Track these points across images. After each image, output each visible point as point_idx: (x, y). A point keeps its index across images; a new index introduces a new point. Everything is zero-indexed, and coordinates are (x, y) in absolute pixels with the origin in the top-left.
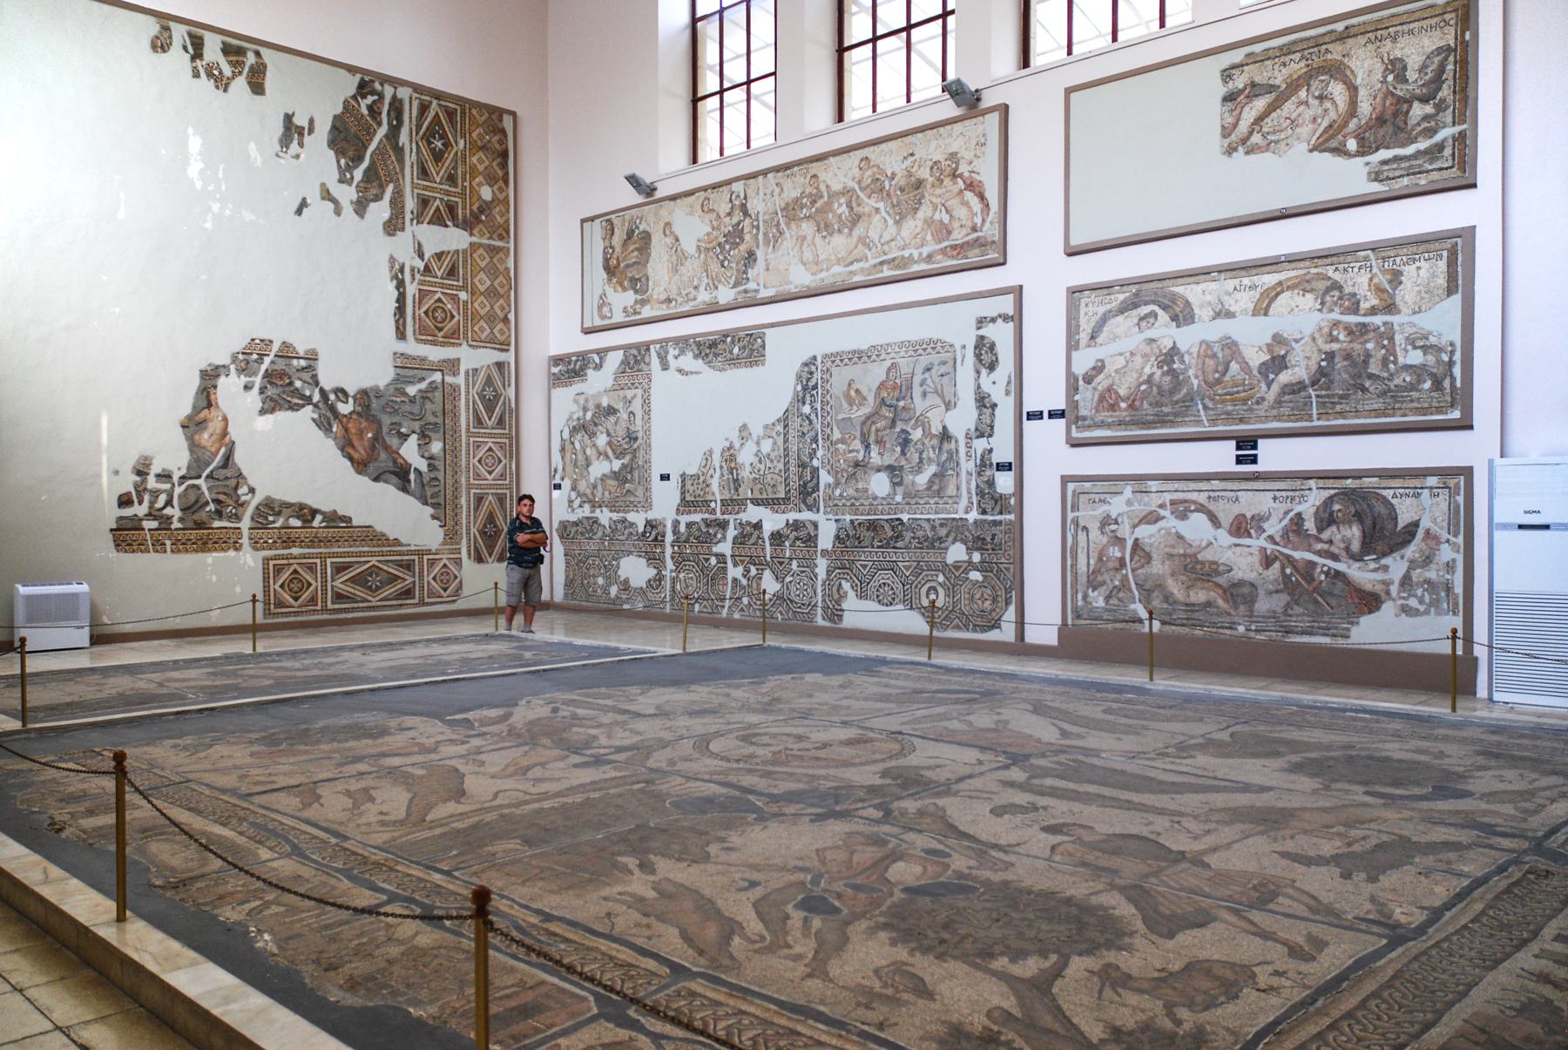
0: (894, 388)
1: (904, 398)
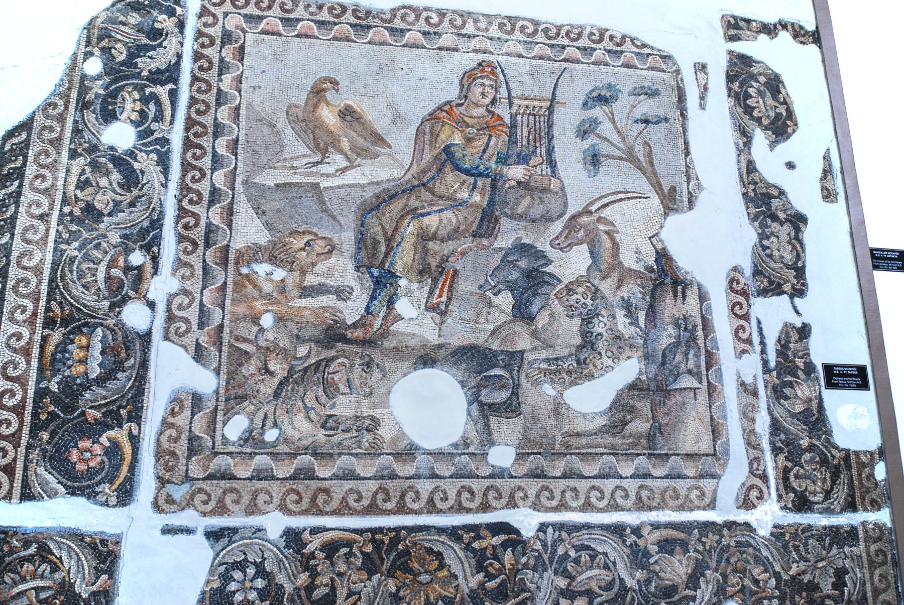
0: (488, 128)
1: (523, 159)
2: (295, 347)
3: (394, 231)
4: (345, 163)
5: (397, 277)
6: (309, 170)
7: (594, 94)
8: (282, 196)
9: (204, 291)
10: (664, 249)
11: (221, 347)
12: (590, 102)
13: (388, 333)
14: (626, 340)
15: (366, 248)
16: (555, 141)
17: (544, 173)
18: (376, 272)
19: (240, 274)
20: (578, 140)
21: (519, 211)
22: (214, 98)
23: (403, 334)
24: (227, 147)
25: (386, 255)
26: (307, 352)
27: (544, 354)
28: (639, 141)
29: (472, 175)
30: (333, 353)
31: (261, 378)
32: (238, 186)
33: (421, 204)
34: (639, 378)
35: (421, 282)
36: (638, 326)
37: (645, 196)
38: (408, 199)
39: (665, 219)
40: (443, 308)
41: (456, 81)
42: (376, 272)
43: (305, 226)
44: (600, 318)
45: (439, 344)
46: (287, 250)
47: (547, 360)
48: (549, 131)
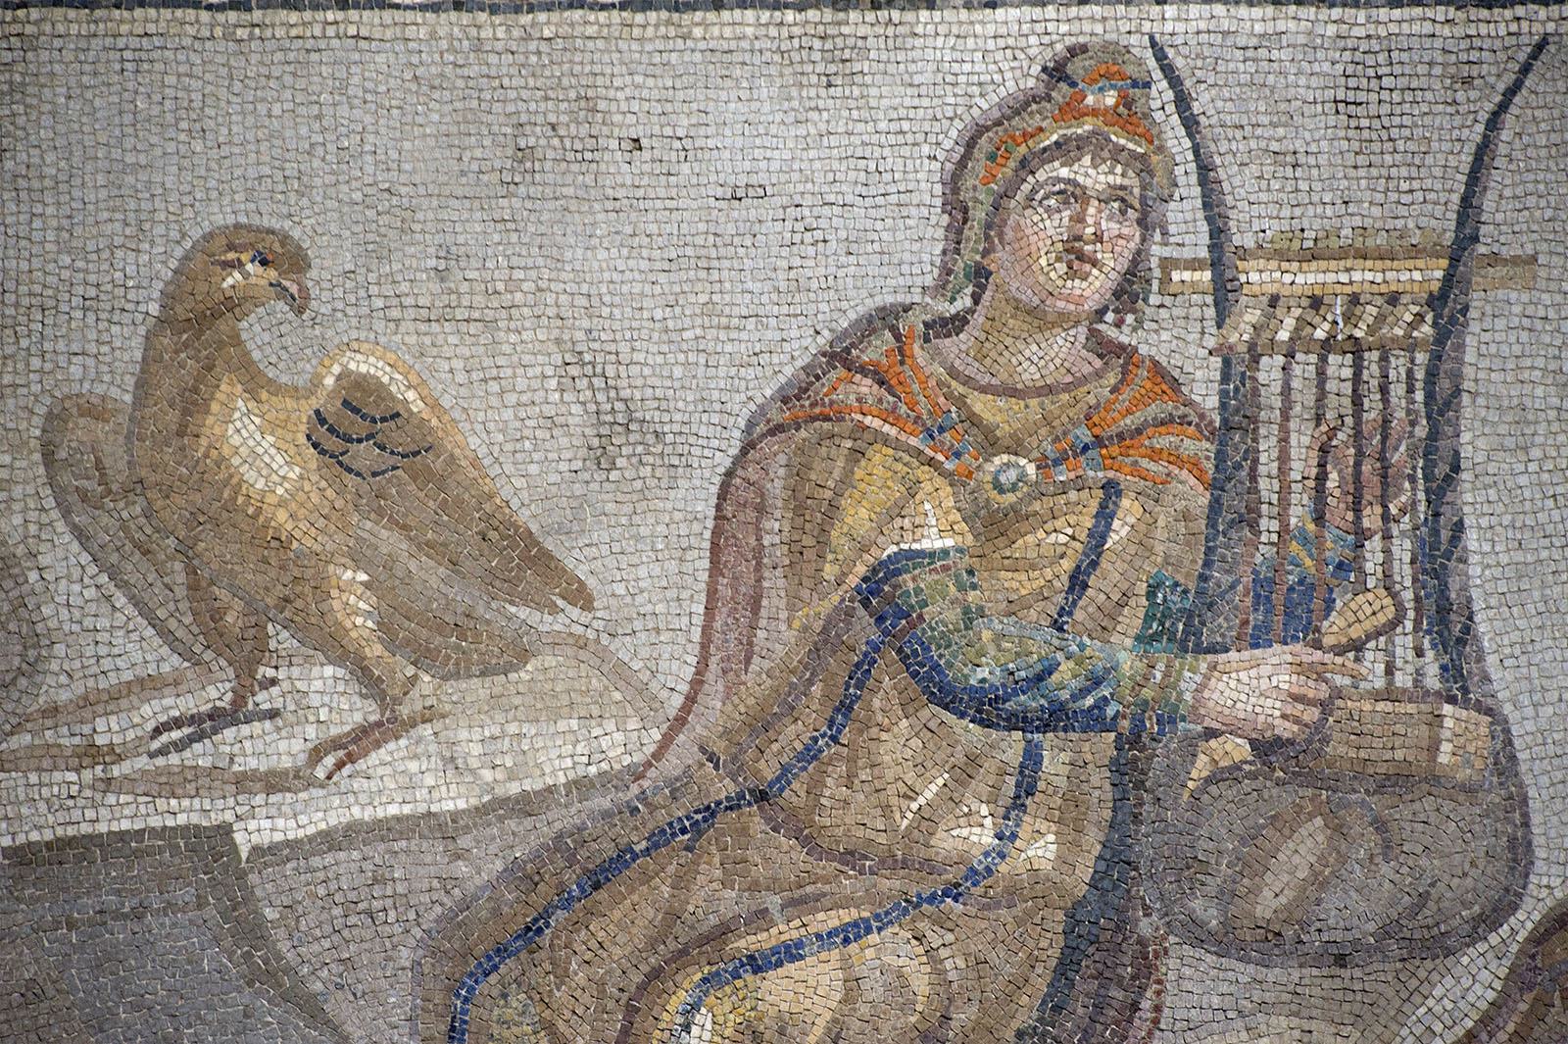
4: (357, 711)
6: (174, 759)
21: (1267, 904)
29: (1018, 722)
33: (747, 905)
38: (682, 882)
41: (928, 188)
48: (1434, 435)
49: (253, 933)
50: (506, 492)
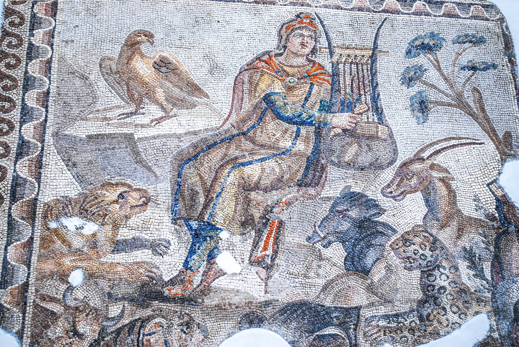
2: (107, 306)
3: (213, 181)
4: (160, 114)
5: (218, 229)
6: (122, 120)
7: (417, 43)
8: (94, 148)
9: (9, 248)
10: (504, 196)
11: (25, 308)
12: (414, 51)
13: (209, 290)
14: (472, 293)
15: (184, 199)
16: (379, 88)
17: (370, 120)
18: (194, 224)
19: (49, 229)
20: (404, 87)
21: (347, 159)
22: (25, 52)
23: (225, 291)
24: (38, 99)
25: (206, 206)
26: (120, 311)
27: (383, 310)
28: (468, 87)
29: (294, 123)
30: (149, 312)
31: (69, 341)
32: (49, 138)
33: (241, 154)
34: (491, 336)
35: (244, 234)
36: (483, 278)
37: (479, 142)
38: (227, 148)
39: (502, 165)
40: (269, 262)
41: (274, 32)
42: (194, 224)
43: (119, 178)
44: (441, 270)
45: (266, 301)
46: (99, 203)
47: (386, 317)
48: (372, 79)
49: (137, 153)
50: (192, 77)
